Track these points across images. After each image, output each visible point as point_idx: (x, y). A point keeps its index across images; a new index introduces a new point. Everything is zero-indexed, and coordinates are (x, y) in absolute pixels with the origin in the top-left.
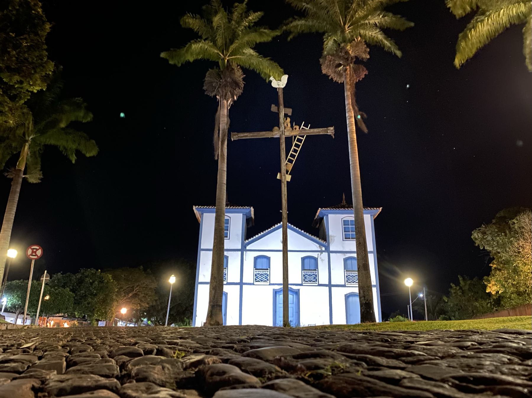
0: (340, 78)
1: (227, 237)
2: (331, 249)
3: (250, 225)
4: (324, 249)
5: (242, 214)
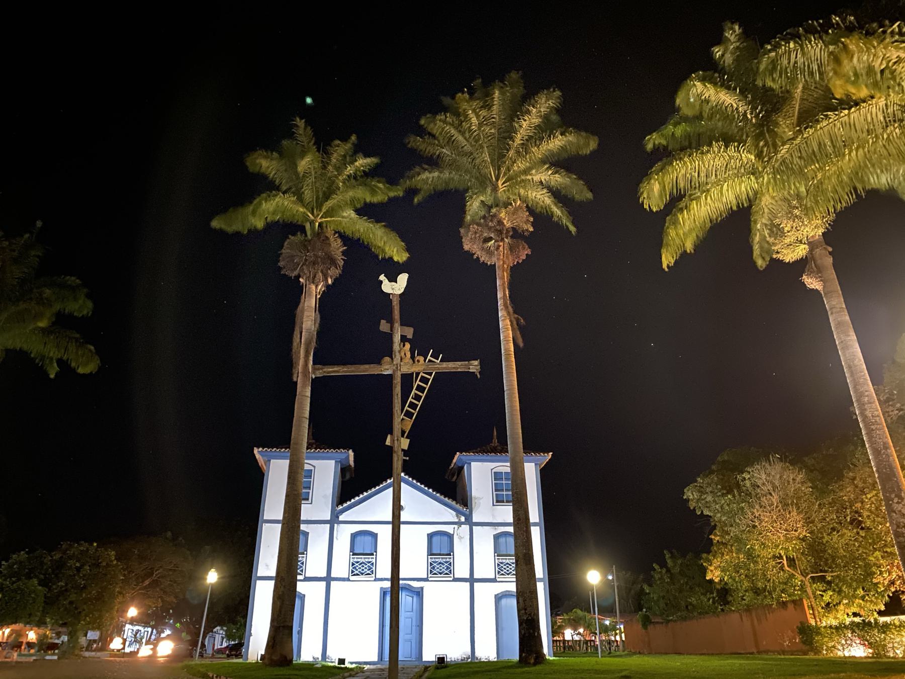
0: (490, 258)
1: (308, 499)
2: (475, 520)
3: (348, 477)
4: (463, 519)
5: (334, 461)
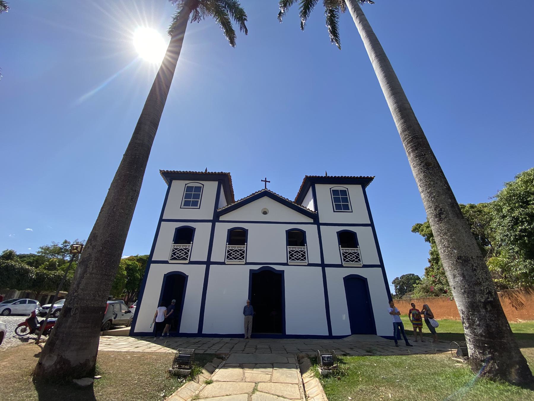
4: (312, 221)
